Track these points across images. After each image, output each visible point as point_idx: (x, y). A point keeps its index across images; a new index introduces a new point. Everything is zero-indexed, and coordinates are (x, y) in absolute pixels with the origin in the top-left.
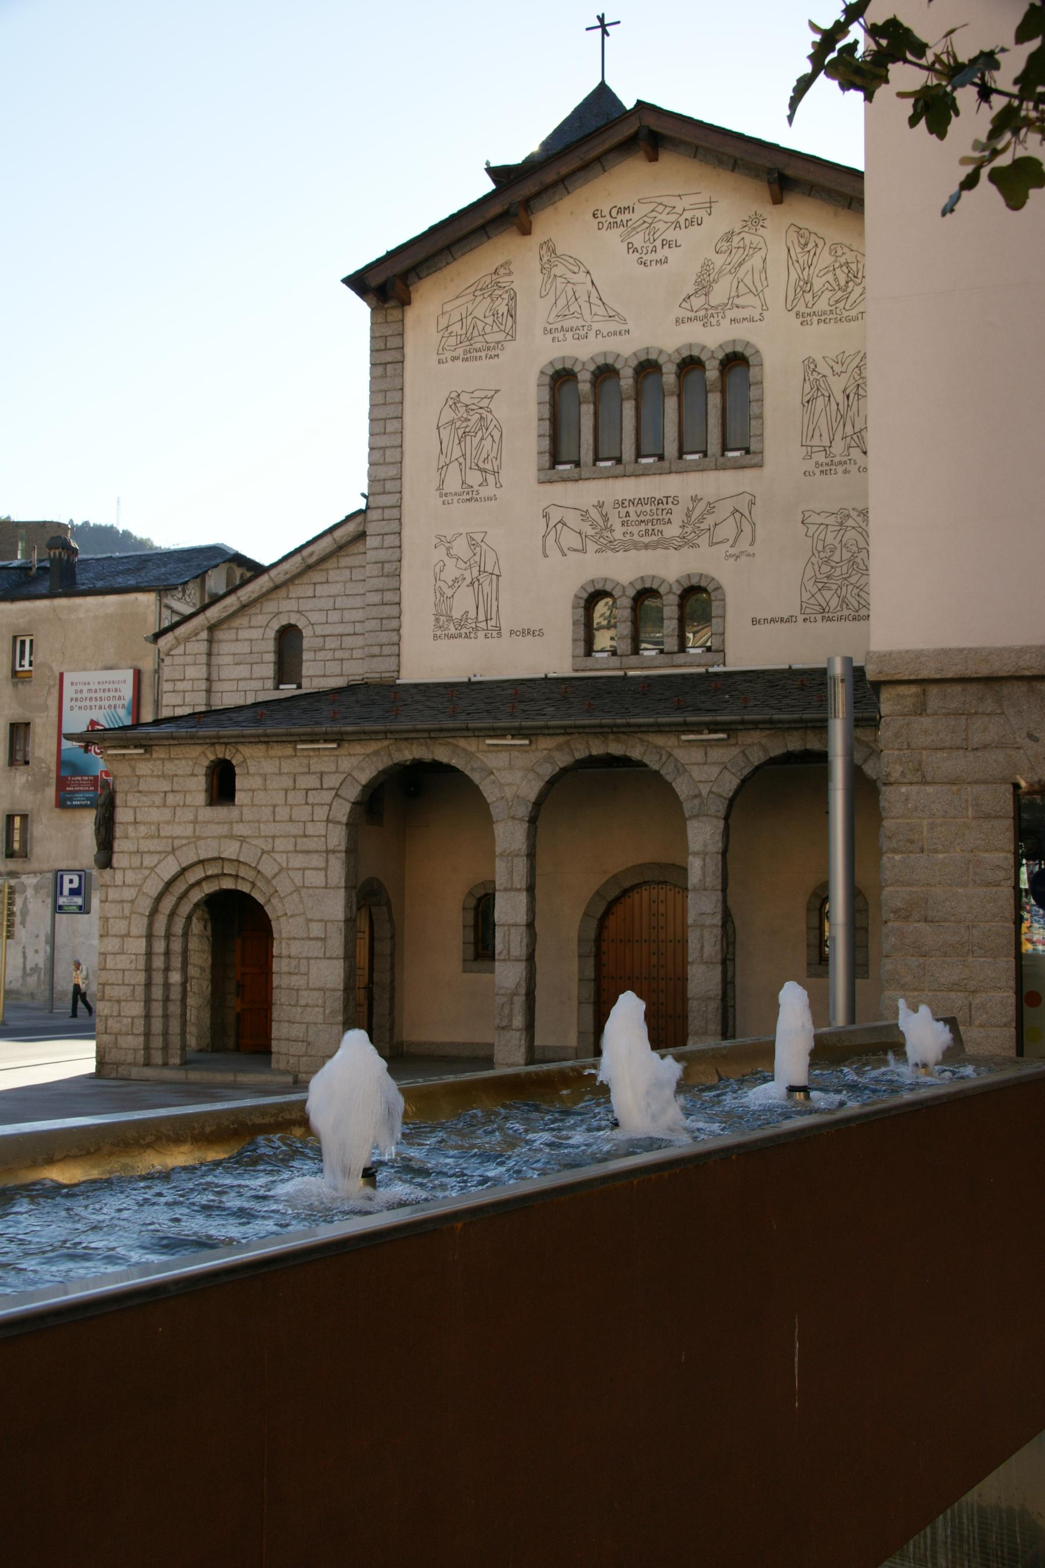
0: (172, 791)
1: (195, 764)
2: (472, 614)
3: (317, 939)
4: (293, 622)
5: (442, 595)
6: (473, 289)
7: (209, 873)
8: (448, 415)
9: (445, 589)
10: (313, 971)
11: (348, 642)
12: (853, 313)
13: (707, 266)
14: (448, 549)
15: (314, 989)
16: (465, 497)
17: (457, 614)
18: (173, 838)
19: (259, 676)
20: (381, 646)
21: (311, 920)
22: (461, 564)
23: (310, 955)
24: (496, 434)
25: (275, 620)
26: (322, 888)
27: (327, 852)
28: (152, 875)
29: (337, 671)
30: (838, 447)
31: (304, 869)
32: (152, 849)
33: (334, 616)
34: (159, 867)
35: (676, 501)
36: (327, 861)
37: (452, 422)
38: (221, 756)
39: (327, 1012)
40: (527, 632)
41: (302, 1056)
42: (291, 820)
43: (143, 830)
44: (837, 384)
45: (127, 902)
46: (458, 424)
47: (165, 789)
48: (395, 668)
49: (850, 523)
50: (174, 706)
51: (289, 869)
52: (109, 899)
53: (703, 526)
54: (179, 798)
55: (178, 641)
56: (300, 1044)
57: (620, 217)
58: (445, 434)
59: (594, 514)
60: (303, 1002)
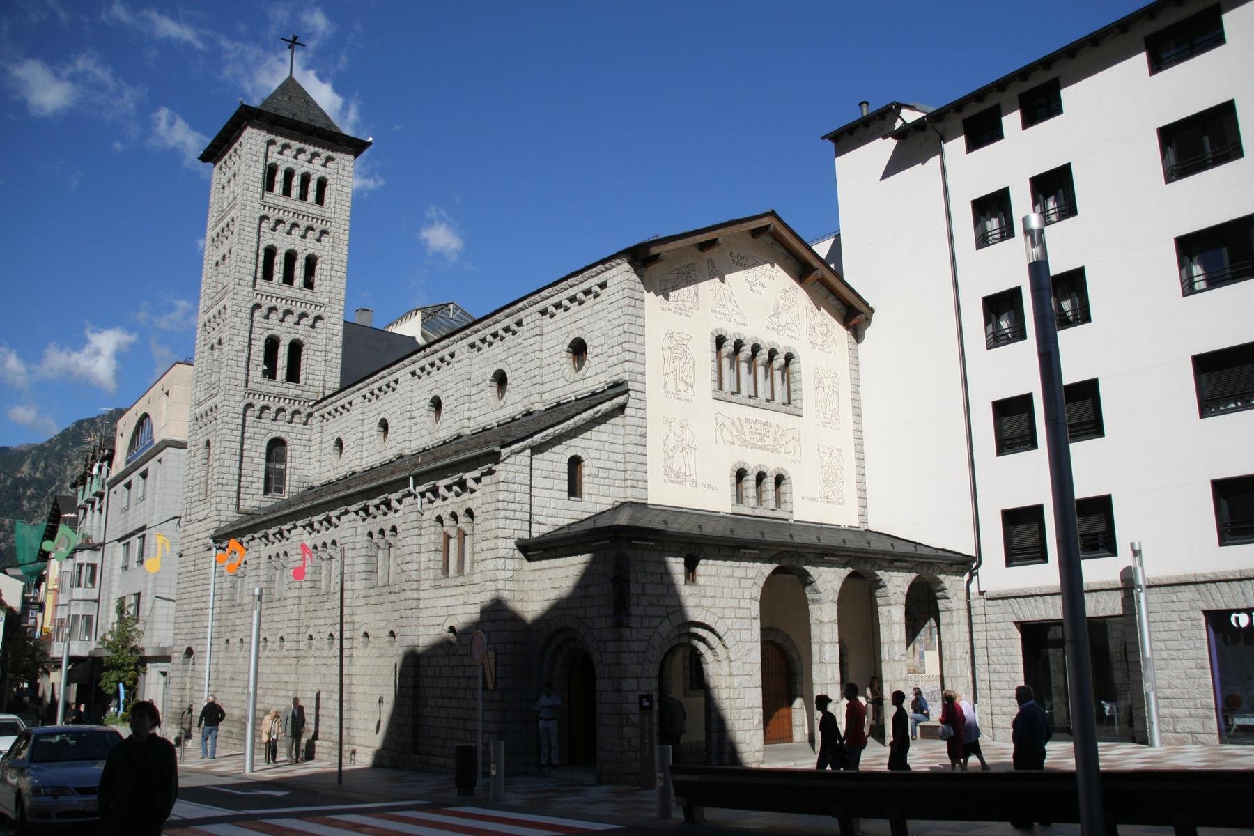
2: (683, 471)
4: (579, 454)
5: (668, 454)
6: (677, 272)
7: (683, 631)
8: (667, 344)
9: (669, 452)
10: (747, 696)
11: (612, 474)
12: (830, 349)
13: (777, 302)
14: (670, 426)
16: (677, 396)
17: (675, 469)
18: (667, 607)
19: (559, 488)
20: (638, 481)
21: (745, 663)
22: (676, 438)
24: (692, 365)
25: (568, 451)
27: (751, 619)
29: (607, 494)
30: (828, 416)
31: (740, 629)
33: (604, 456)
35: (770, 426)
36: (752, 625)
37: (669, 348)
39: (756, 722)
40: (710, 486)
44: (827, 383)
46: (673, 350)
48: (645, 497)
49: (834, 454)
53: (782, 442)
55: (513, 453)
57: (741, 261)
58: (666, 353)
59: (736, 421)
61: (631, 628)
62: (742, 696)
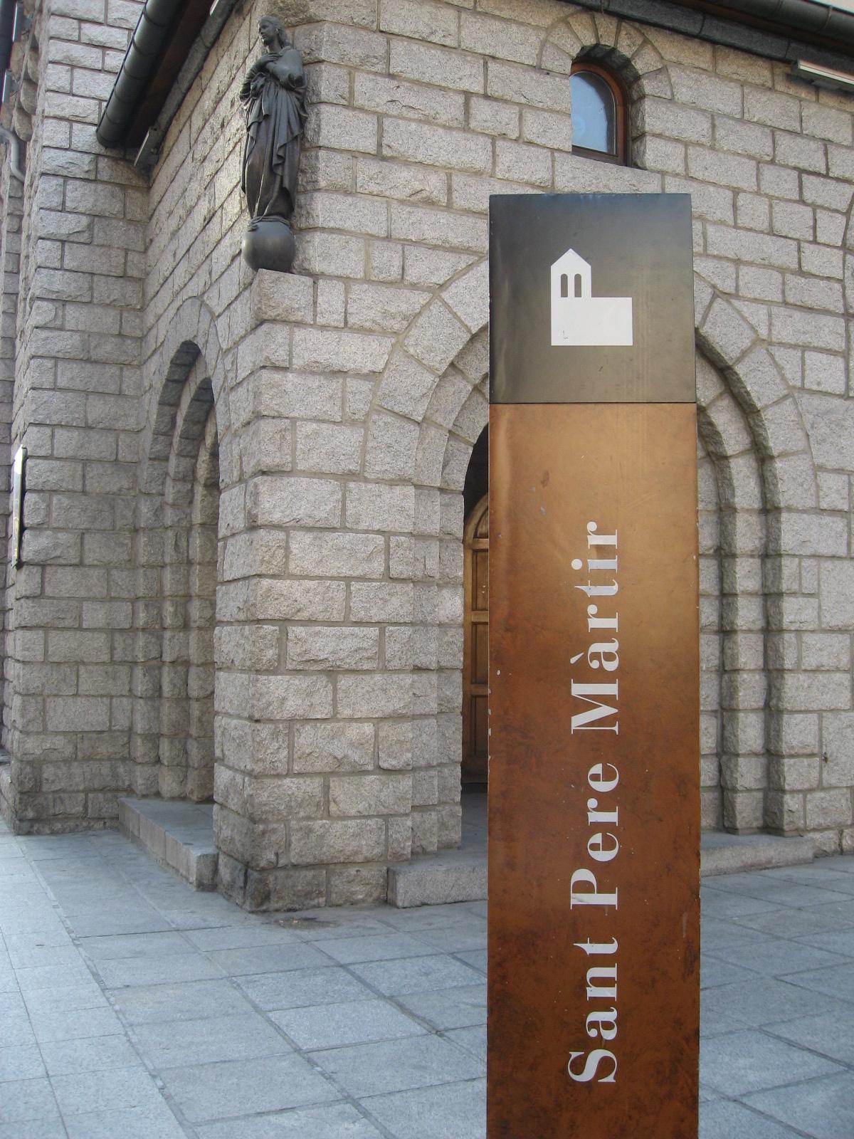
0: (486, 96)
1: (543, 44)
3: (834, 512)
15: (832, 631)
23: (823, 550)
26: (840, 396)
28: (435, 308)
32: (431, 235)
34: (452, 289)
38: (608, 41)
41: (811, 790)
42: (772, 232)
43: (404, 180)
45: (358, 375)
47: (465, 85)
50: (81, 20)
51: (771, 344)
52: (297, 363)
54: (507, 116)
56: (806, 761)
60: (811, 661)
61: (315, 277)
62: (809, 584)
